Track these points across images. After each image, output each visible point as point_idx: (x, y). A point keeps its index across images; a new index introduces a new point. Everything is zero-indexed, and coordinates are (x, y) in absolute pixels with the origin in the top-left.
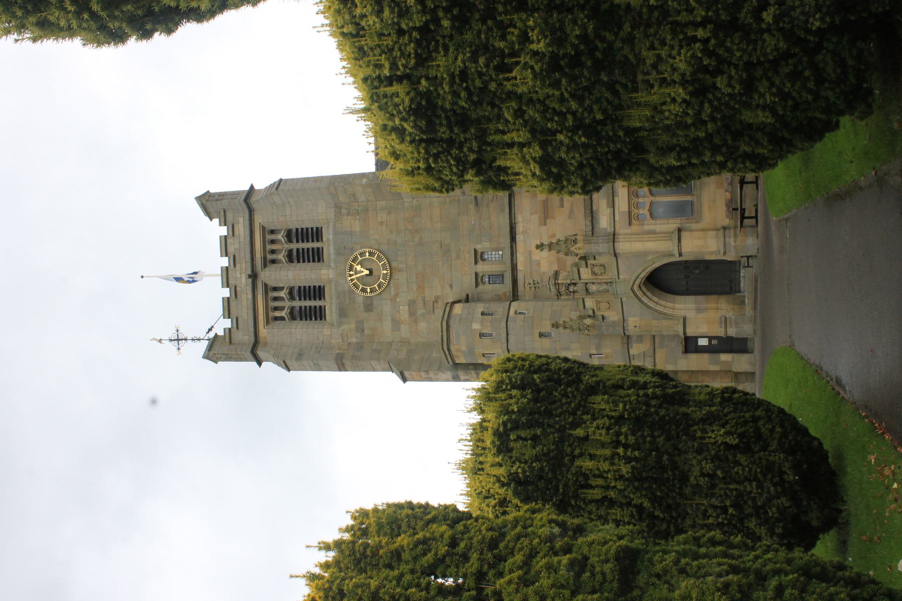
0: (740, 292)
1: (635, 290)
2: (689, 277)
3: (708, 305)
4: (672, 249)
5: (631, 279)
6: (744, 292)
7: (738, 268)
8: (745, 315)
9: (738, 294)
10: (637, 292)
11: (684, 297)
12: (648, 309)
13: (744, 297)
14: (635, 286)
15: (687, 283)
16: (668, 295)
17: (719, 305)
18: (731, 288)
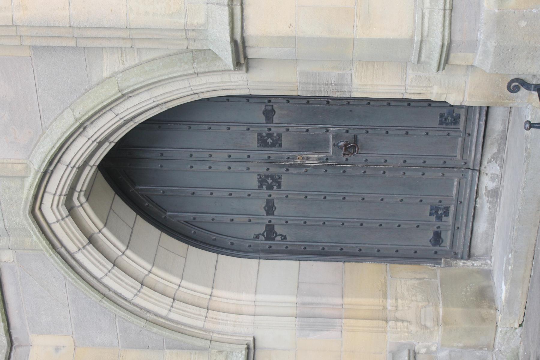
0: (470, 256)
1: (51, 217)
2: (277, 182)
3: (347, 300)
4: (199, 20)
5: (27, 167)
6: (487, 254)
7: (472, 157)
8: (491, 347)
9: (461, 263)
10: (57, 228)
11: (252, 263)
12: (106, 303)
13: (488, 274)
14: (48, 199)
15: (270, 208)
16: (195, 252)
17: (390, 303)
18: (437, 238)
